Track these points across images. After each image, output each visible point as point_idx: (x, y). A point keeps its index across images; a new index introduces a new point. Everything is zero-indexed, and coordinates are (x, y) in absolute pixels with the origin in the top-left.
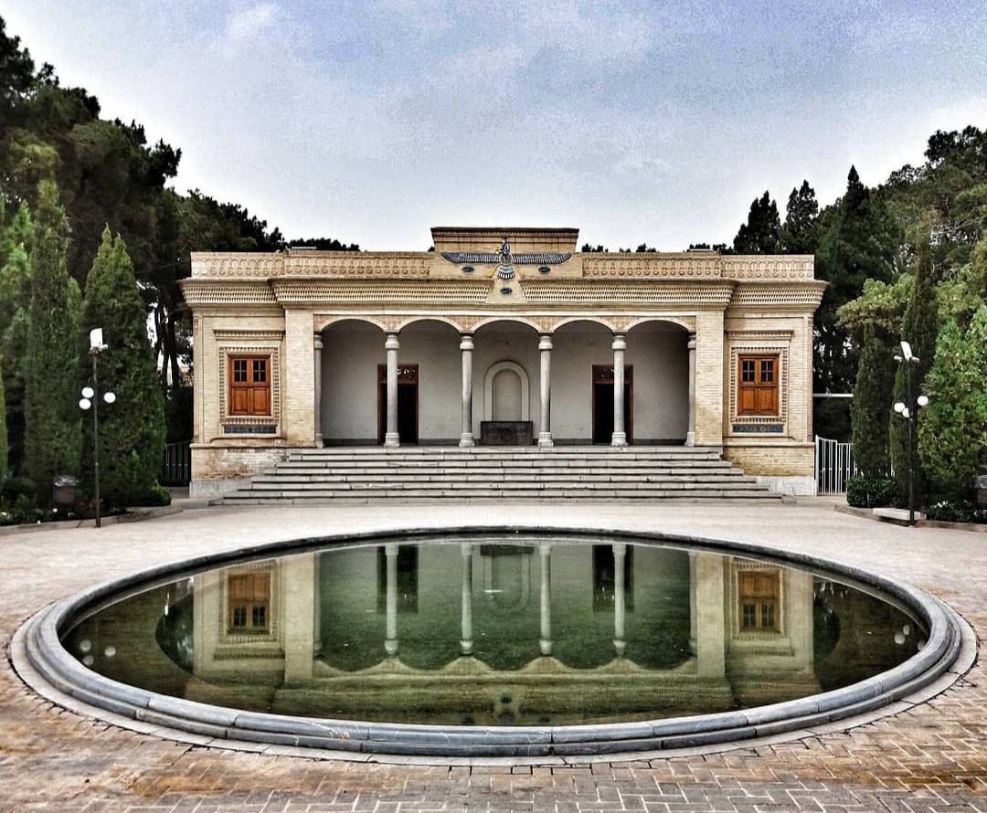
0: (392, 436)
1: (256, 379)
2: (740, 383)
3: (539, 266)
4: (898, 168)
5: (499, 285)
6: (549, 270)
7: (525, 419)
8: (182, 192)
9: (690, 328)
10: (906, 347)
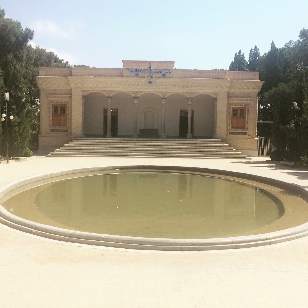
0: (109, 133)
1: (61, 112)
2: (232, 117)
3: (162, 74)
4: (288, 41)
5: (148, 80)
6: (166, 75)
7: (155, 128)
8: (34, 47)
9: (215, 97)
10: (295, 104)
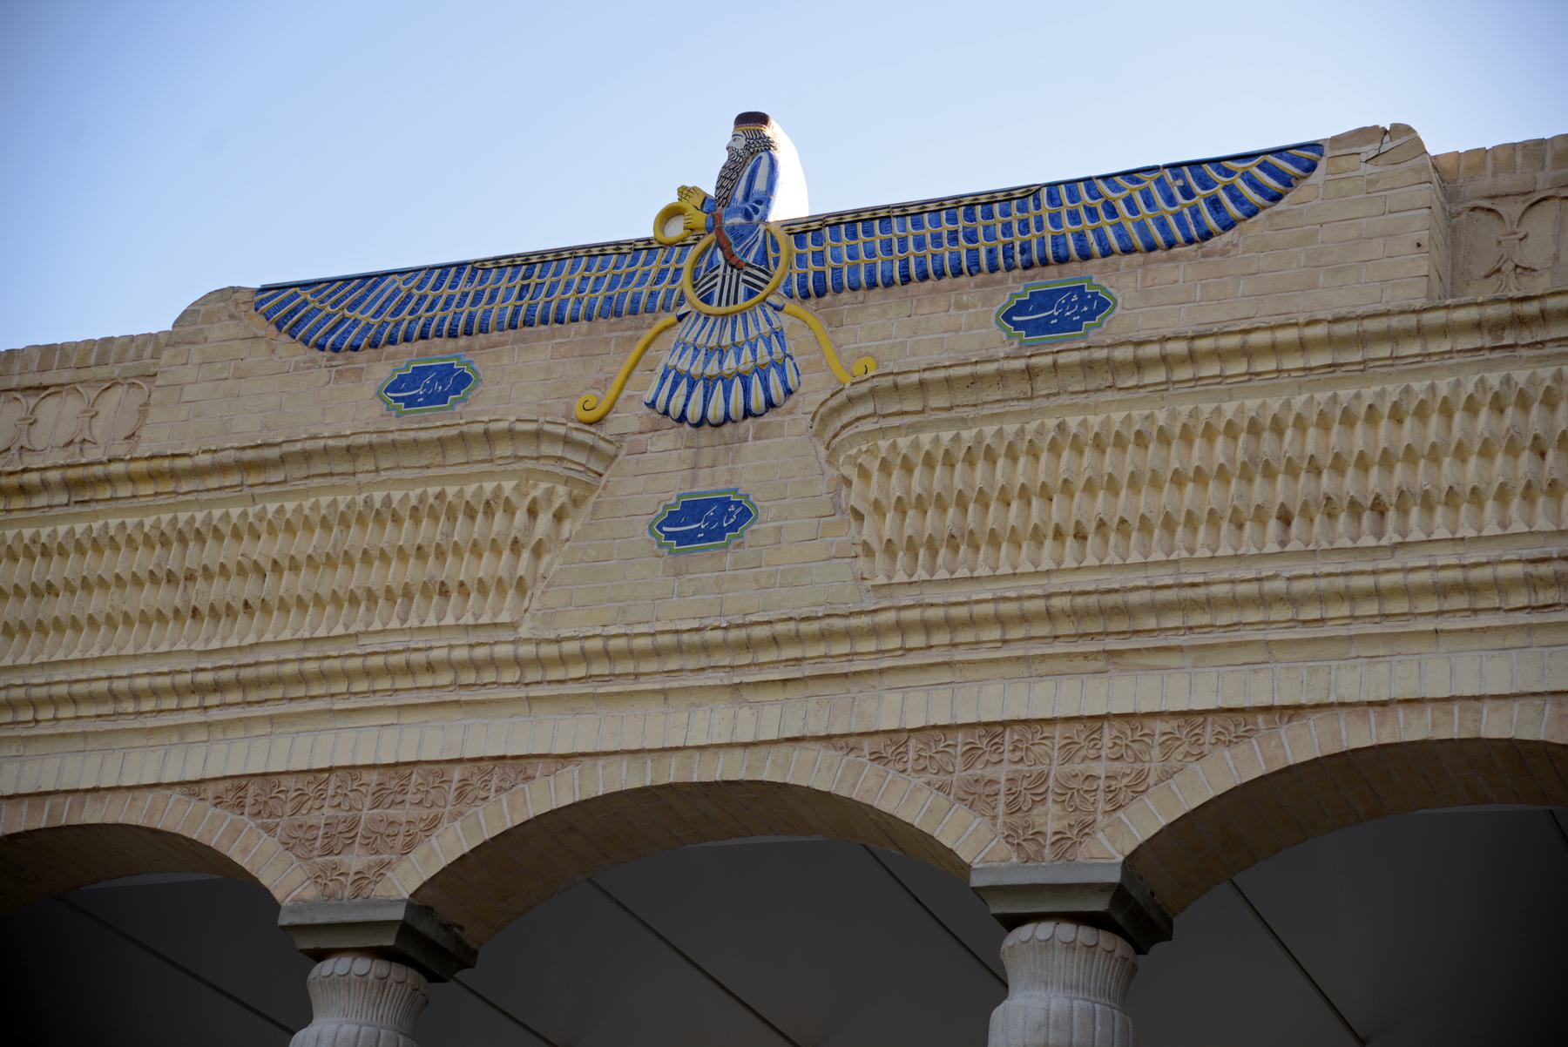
5: (666, 471)
6: (1096, 305)
